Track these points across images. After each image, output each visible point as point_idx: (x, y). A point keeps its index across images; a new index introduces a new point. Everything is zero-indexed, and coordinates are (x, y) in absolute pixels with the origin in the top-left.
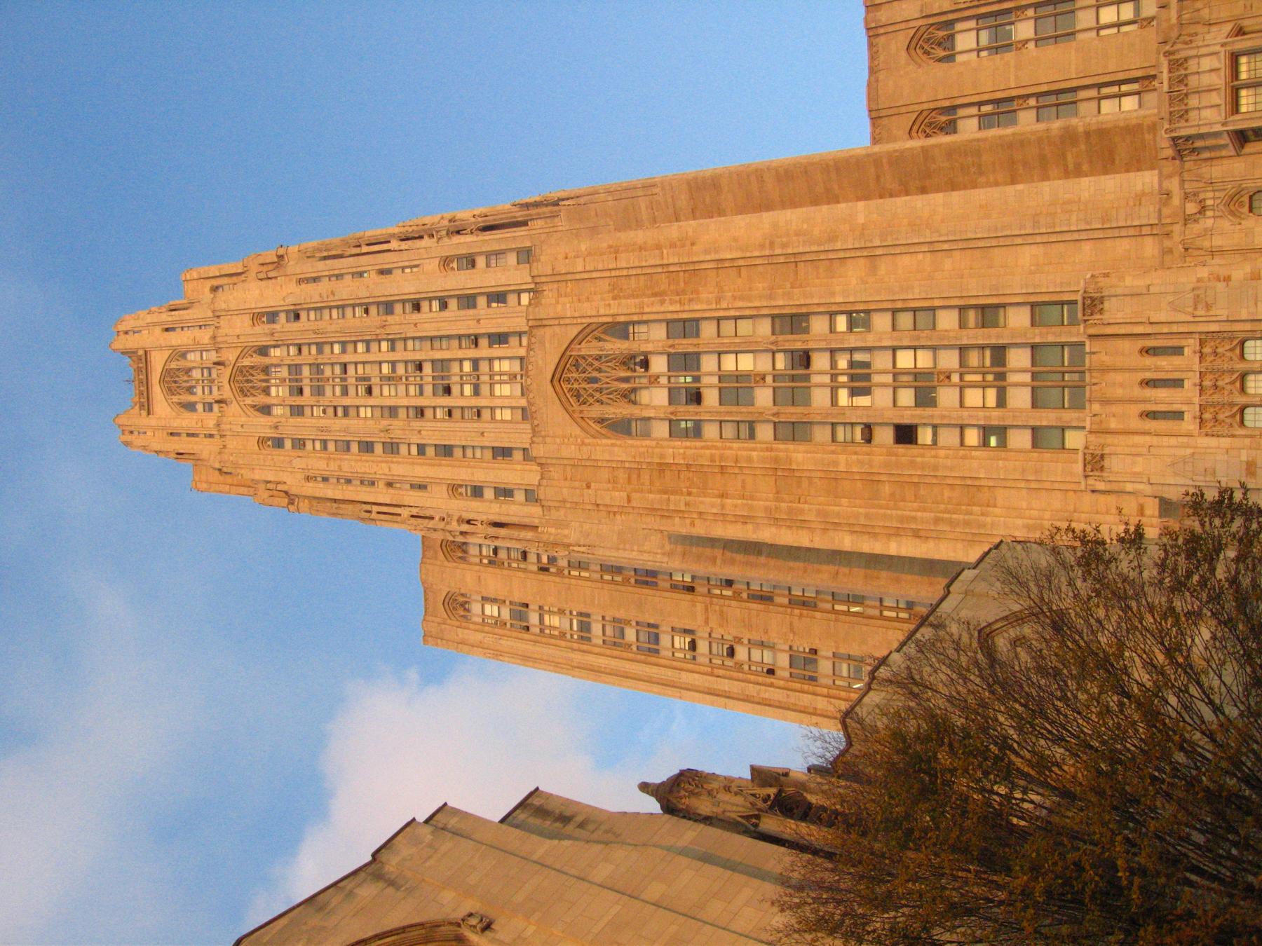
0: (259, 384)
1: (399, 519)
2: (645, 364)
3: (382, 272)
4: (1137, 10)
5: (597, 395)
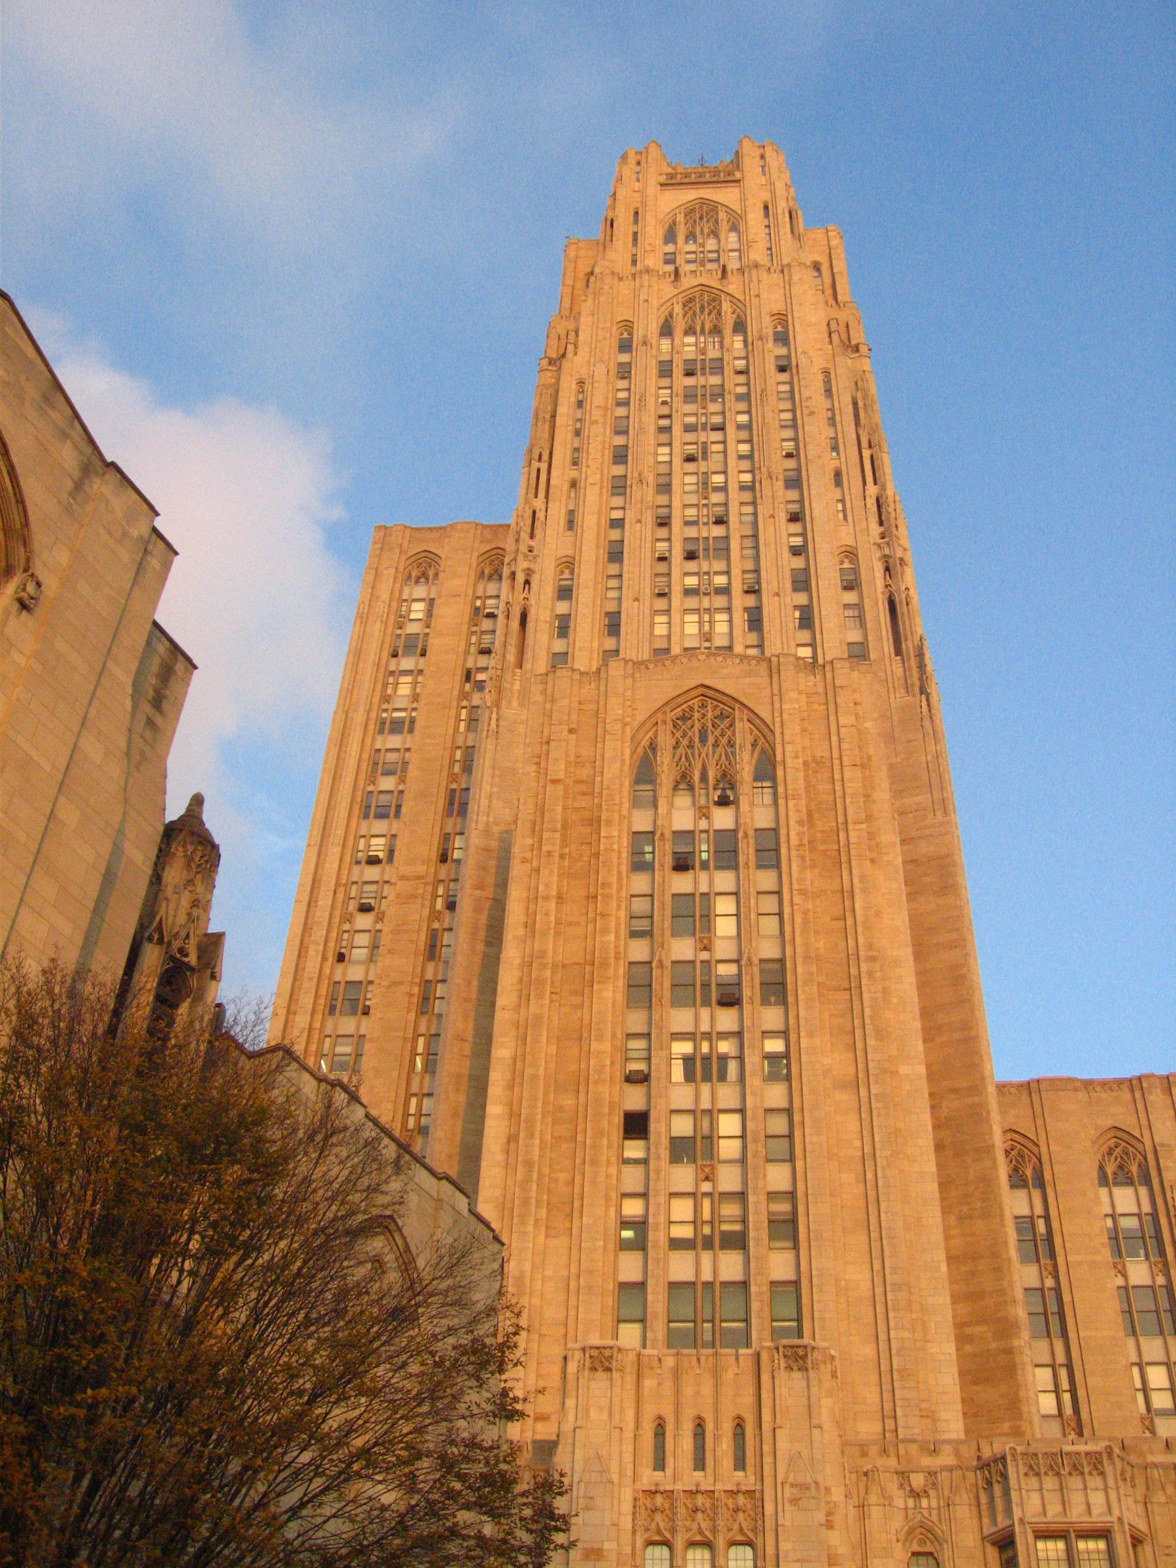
0: (699, 322)
1: (531, 495)
2: (723, 802)
3: (838, 475)
4: (1164, 1413)
5: (685, 742)
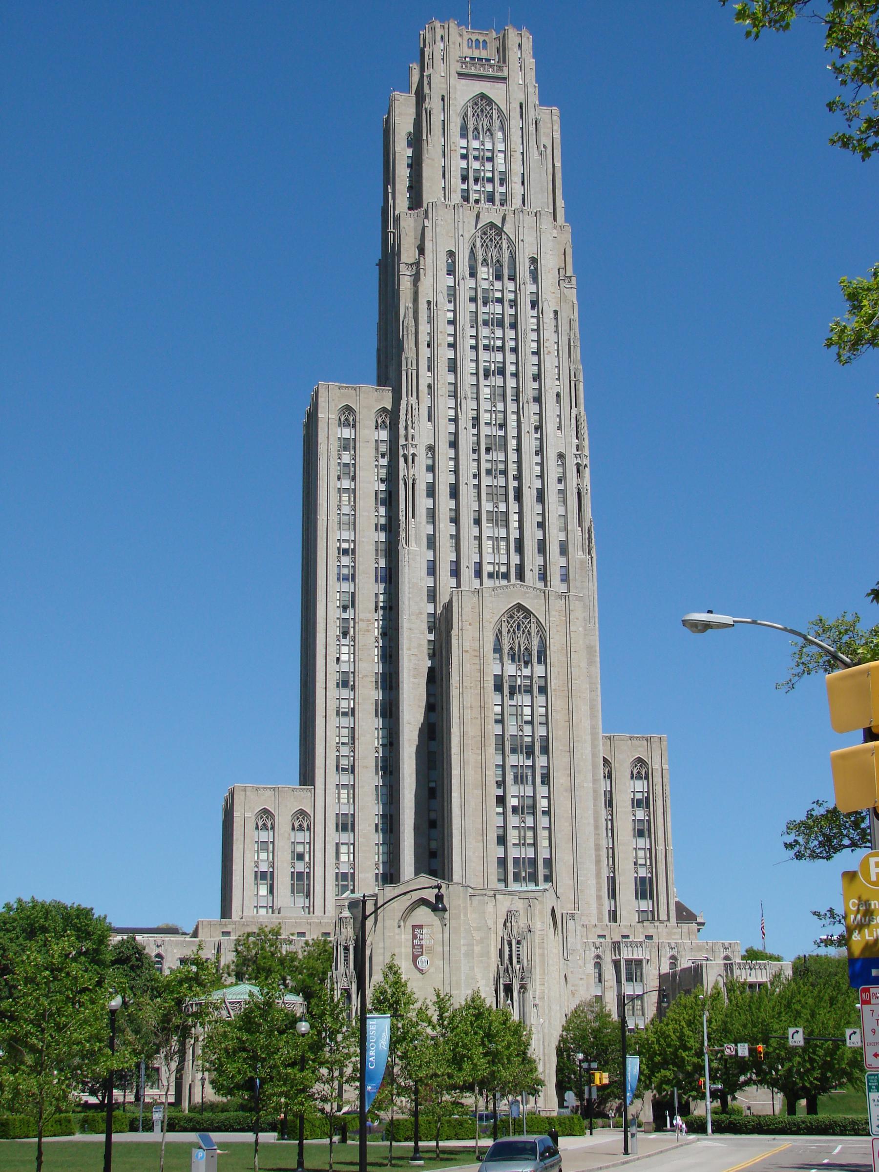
3: (558, 395)
